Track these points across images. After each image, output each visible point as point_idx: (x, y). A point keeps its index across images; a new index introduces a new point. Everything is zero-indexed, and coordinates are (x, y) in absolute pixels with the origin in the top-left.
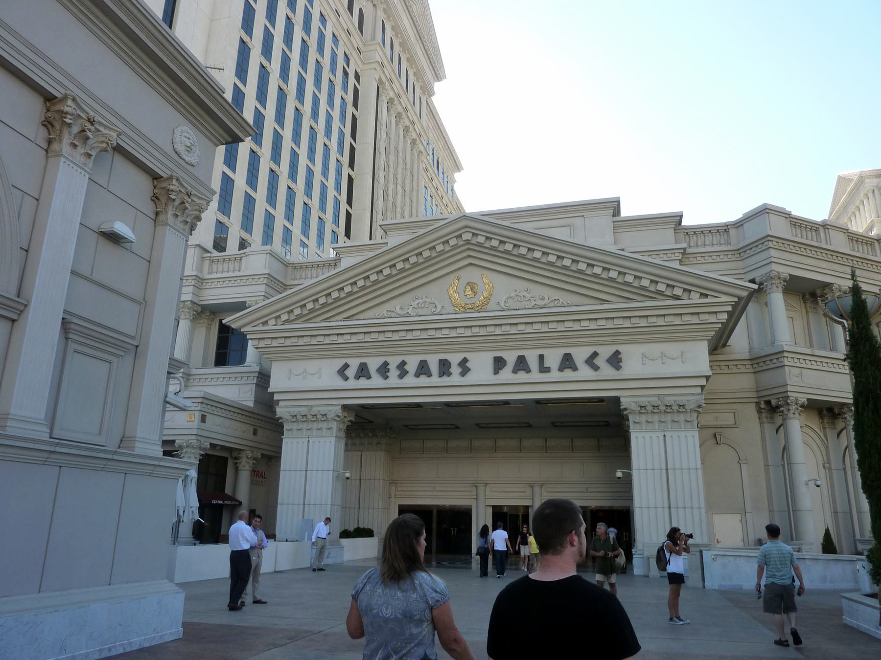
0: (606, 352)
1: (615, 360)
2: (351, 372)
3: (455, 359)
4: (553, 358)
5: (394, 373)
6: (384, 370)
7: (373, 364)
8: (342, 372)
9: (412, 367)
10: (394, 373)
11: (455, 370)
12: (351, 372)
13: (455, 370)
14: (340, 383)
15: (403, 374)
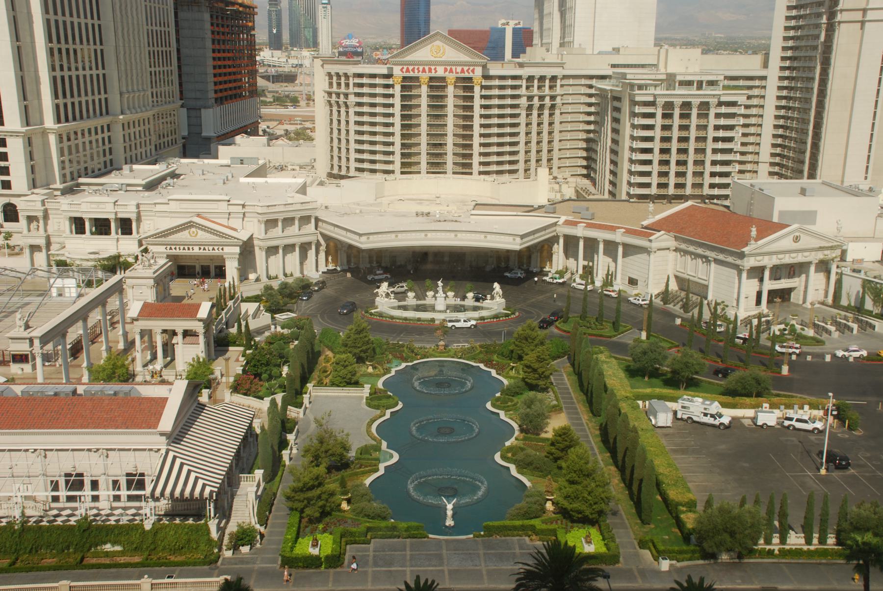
0: (471, 68)
1: (473, 71)
2: (404, 70)
3: (433, 68)
4: (459, 69)
5: (416, 71)
6: (413, 70)
7: (411, 68)
8: (402, 70)
9: (421, 69)
10: (416, 71)
11: (433, 71)
12: (404, 70)
13: (433, 71)
14: (401, 73)
15: (419, 72)
